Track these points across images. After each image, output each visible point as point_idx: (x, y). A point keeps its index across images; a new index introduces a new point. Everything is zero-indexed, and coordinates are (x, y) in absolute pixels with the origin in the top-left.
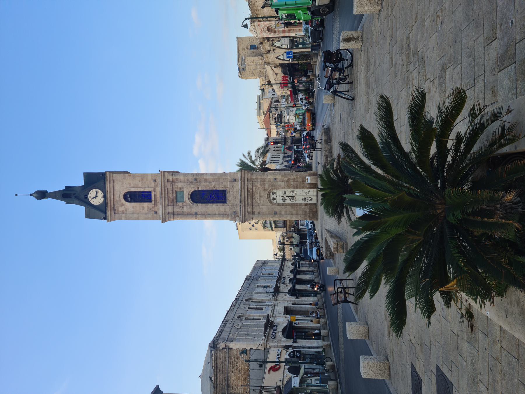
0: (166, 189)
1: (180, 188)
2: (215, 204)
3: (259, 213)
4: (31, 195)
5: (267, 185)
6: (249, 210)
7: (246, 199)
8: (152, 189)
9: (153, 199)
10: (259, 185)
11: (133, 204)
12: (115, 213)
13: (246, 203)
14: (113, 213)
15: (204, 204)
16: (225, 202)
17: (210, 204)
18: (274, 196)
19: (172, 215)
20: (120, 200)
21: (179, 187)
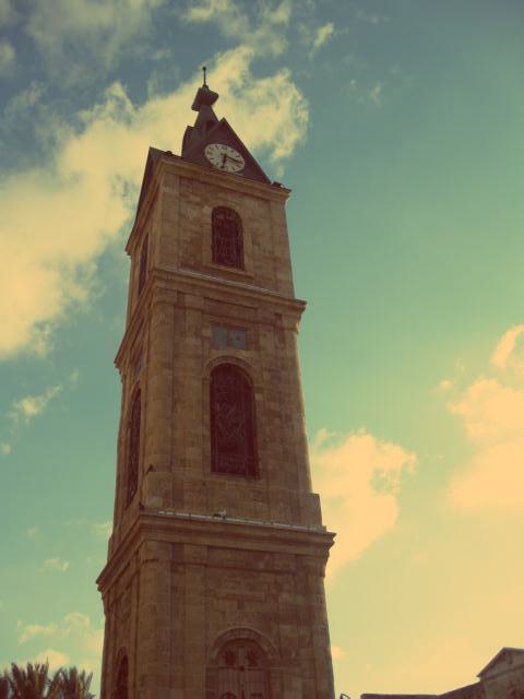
0: (256, 306)
1: (257, 342)
2: (208, 433)
3: (174, 589)
4: (205, 86)
5: (286, 629)
6: (188, 550)
7: (231, 543)
8: (249, 274)
9: (222, 268)
10: (285, 596)
11: (209, 221)
12: (181, 177)
13: (219, 542)
14: (183, 173)
15: (207, 399)
16: (217, 468)
17: (207, 417)
18: (242, 660)
19: (175, 300)
20: (216, 199)
21: (263, 342)
